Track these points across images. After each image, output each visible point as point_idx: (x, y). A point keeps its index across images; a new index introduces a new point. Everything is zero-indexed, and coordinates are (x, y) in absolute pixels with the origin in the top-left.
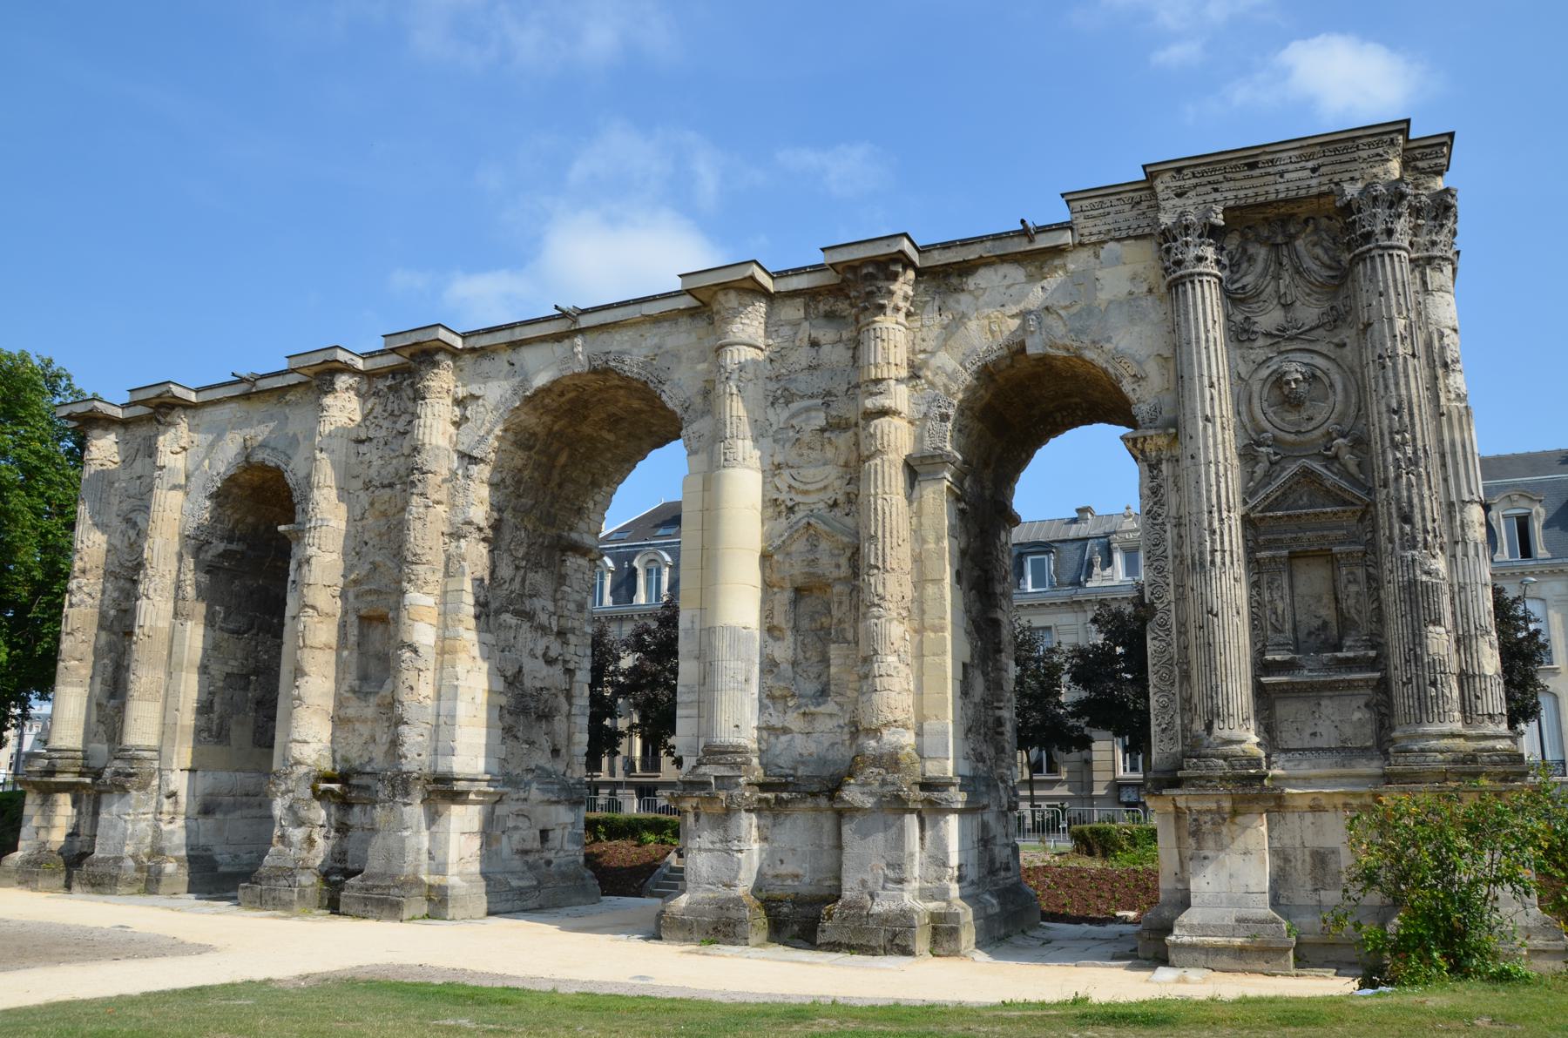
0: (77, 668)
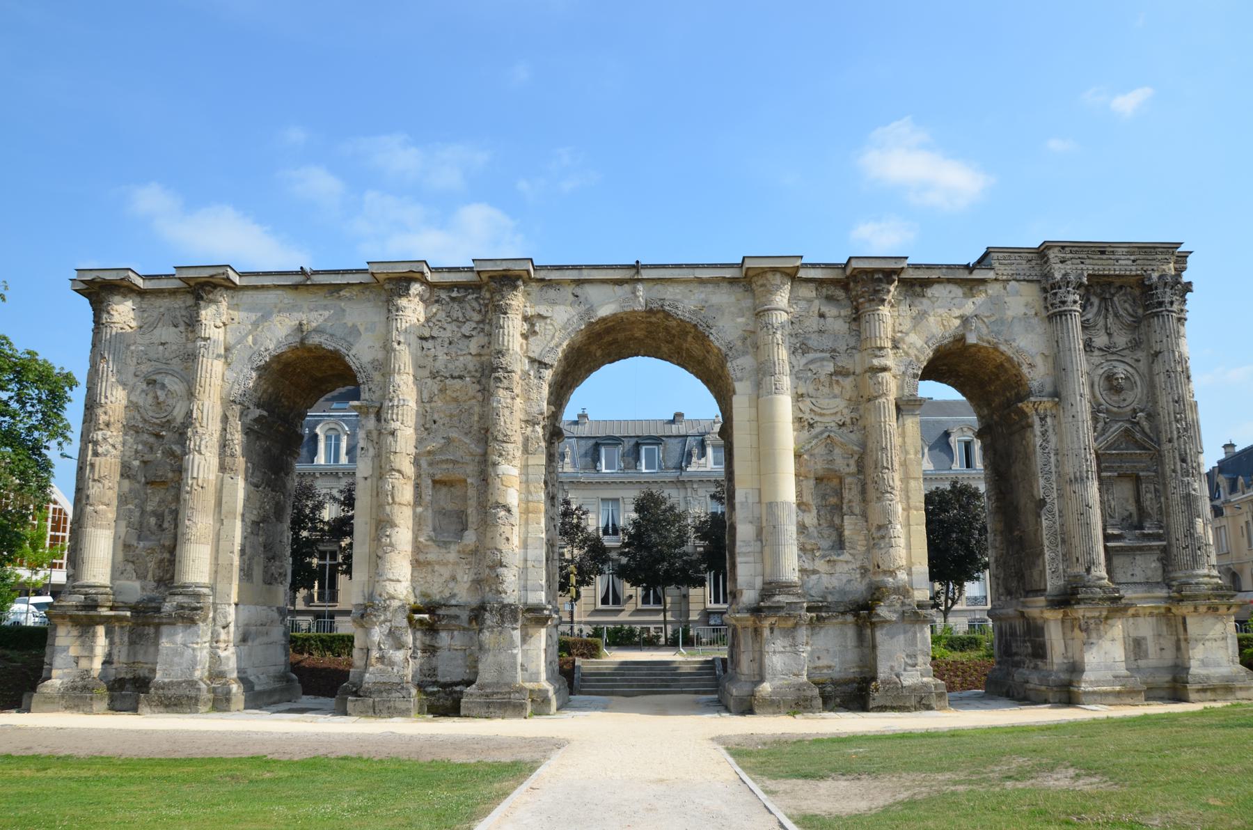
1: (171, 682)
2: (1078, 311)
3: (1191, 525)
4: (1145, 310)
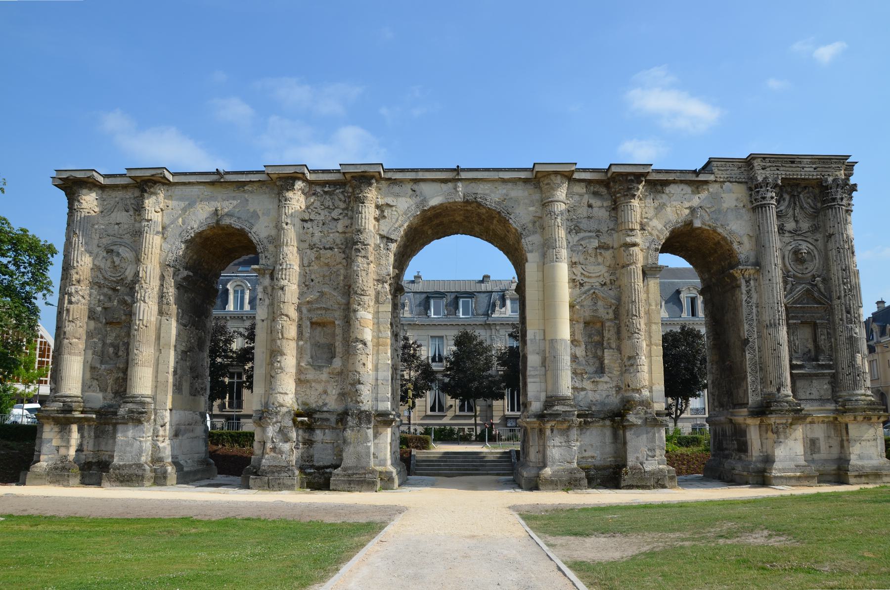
0: (77, 344)
1: (125, 464)
2: (774, 204)
3: (853, 358)
4: (823, 204)
